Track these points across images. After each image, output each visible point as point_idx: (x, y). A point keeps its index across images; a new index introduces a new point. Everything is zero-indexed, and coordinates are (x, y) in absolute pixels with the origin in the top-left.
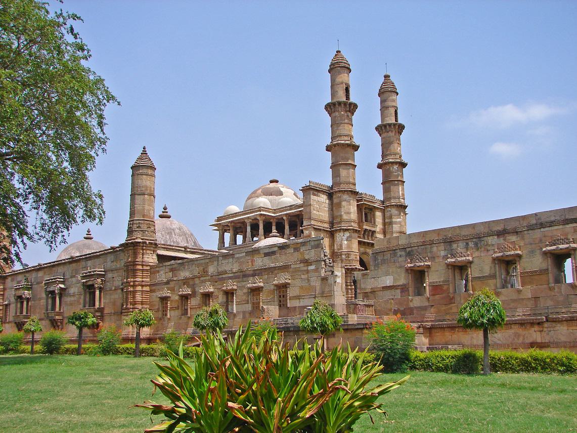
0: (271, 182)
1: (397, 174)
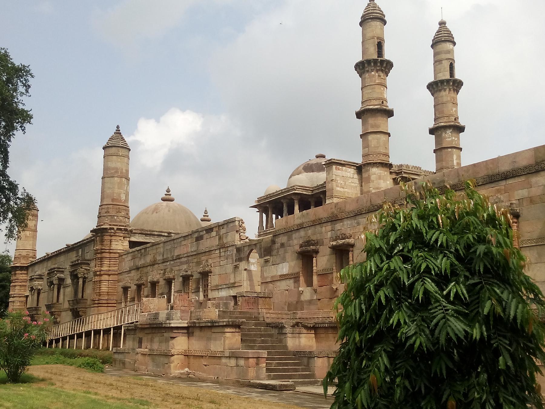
0: (317, 157)
1: (450, 139)
